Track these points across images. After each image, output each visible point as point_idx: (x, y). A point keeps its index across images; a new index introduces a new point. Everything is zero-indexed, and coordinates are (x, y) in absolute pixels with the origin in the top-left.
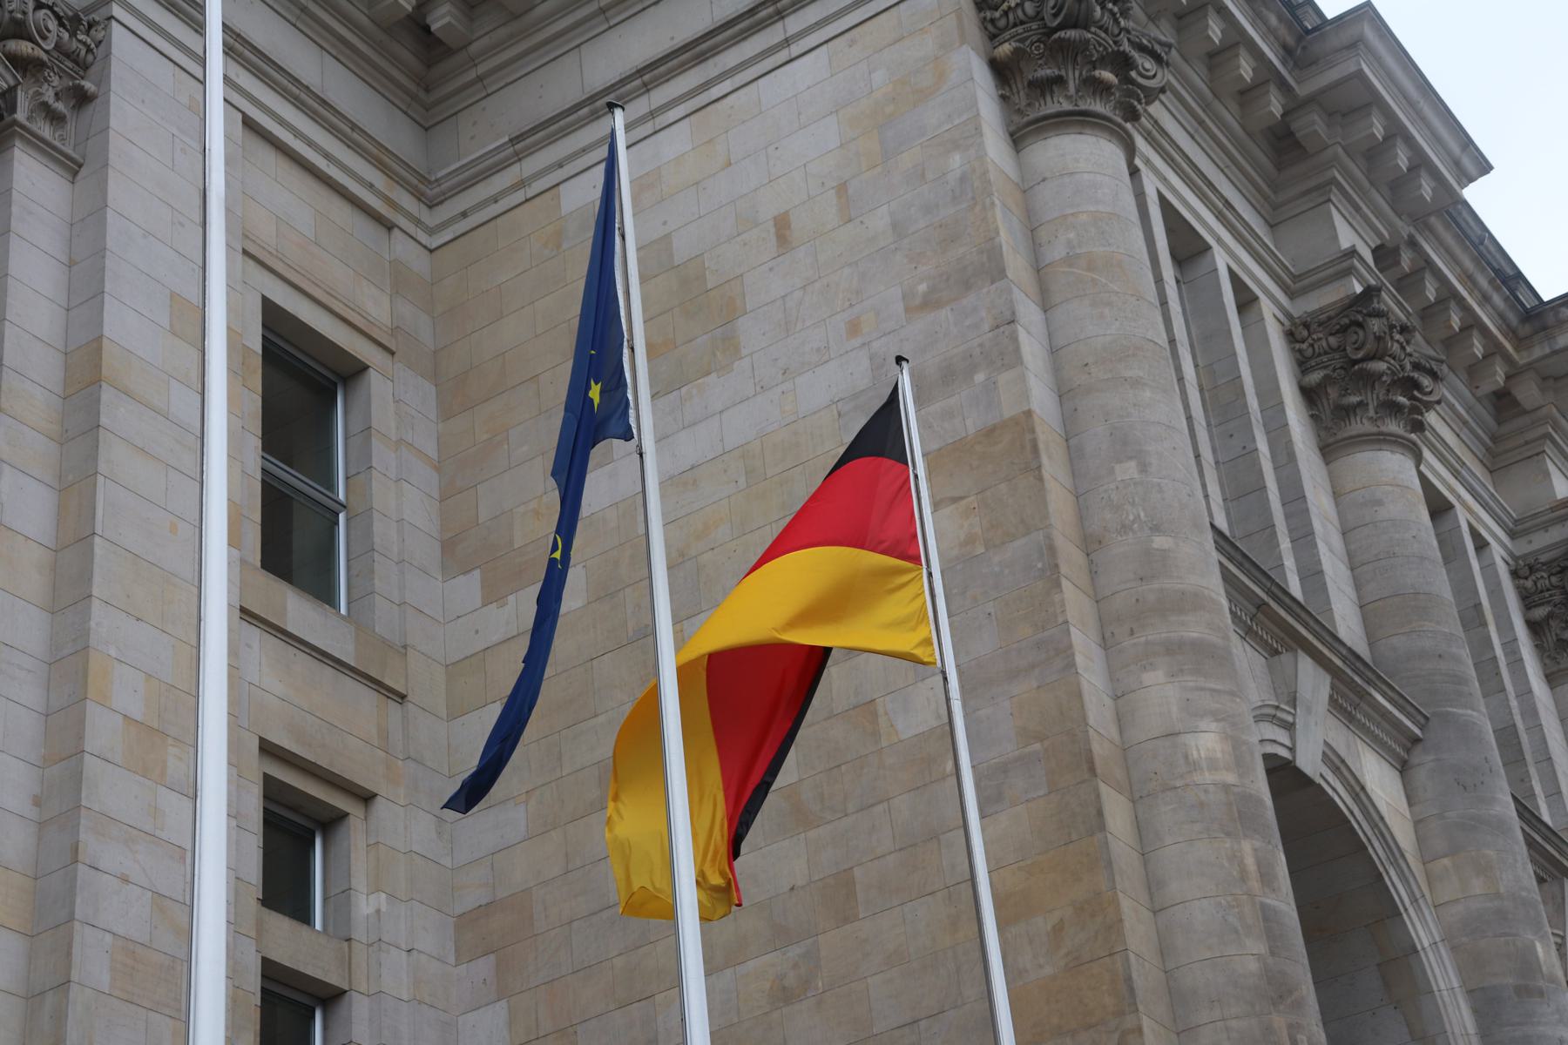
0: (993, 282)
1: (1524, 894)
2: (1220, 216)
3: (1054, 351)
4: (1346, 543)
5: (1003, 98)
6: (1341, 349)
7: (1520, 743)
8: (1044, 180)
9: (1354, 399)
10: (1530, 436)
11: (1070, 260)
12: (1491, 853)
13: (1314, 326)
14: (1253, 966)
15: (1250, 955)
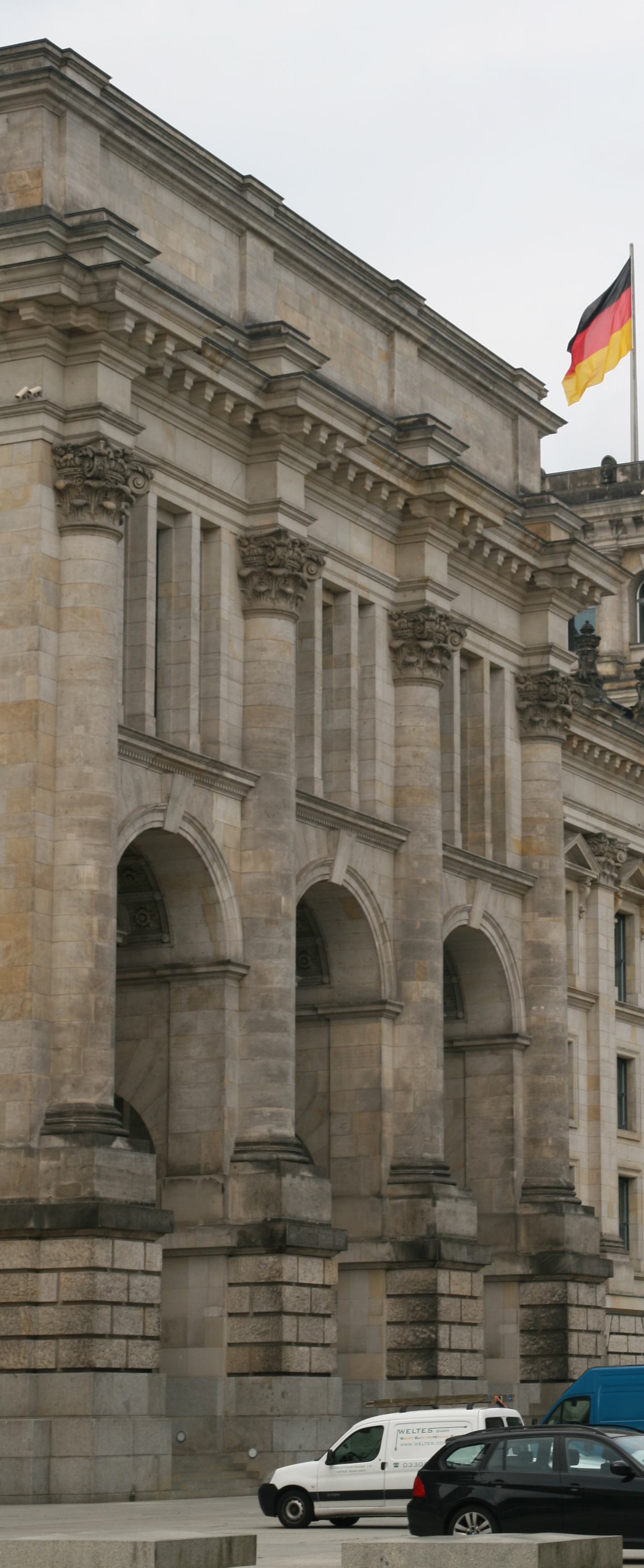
0: (32, 624)
1: (283, 872)
2: (201, 490)
3: (58, 657)
4: (245, 668)
5: (59, 506)
6: (264, 555)
7: (350, 740)
8: (70, 559)
9: (263, 588)
10: (418, 531)
11: (74, 609)
12: (272, 851)
13: (252, 540)
14: (86, 972)
15: (86, 968)
